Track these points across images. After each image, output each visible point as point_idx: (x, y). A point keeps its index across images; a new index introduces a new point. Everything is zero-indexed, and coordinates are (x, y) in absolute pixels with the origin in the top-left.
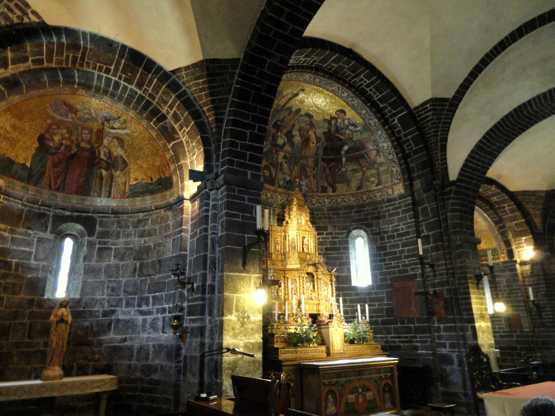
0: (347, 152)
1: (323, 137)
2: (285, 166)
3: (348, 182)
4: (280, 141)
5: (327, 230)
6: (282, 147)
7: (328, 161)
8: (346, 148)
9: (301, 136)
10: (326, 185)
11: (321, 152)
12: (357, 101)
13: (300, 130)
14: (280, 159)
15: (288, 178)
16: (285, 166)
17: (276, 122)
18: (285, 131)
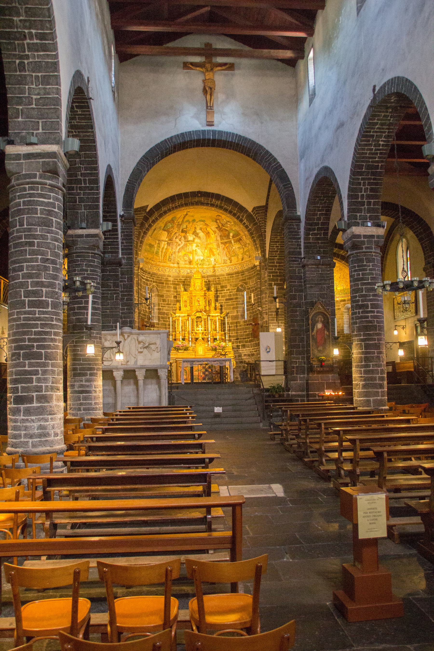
0: (233, 237)
1: (216, 230)
2: (199, 251)
8: (231, 235)
9: (203, 232)
11: (219, 238)
12: (221, 211)
15: (202, 258)
16: (199, 251)
17: (182, 230)
18: (191, 232)
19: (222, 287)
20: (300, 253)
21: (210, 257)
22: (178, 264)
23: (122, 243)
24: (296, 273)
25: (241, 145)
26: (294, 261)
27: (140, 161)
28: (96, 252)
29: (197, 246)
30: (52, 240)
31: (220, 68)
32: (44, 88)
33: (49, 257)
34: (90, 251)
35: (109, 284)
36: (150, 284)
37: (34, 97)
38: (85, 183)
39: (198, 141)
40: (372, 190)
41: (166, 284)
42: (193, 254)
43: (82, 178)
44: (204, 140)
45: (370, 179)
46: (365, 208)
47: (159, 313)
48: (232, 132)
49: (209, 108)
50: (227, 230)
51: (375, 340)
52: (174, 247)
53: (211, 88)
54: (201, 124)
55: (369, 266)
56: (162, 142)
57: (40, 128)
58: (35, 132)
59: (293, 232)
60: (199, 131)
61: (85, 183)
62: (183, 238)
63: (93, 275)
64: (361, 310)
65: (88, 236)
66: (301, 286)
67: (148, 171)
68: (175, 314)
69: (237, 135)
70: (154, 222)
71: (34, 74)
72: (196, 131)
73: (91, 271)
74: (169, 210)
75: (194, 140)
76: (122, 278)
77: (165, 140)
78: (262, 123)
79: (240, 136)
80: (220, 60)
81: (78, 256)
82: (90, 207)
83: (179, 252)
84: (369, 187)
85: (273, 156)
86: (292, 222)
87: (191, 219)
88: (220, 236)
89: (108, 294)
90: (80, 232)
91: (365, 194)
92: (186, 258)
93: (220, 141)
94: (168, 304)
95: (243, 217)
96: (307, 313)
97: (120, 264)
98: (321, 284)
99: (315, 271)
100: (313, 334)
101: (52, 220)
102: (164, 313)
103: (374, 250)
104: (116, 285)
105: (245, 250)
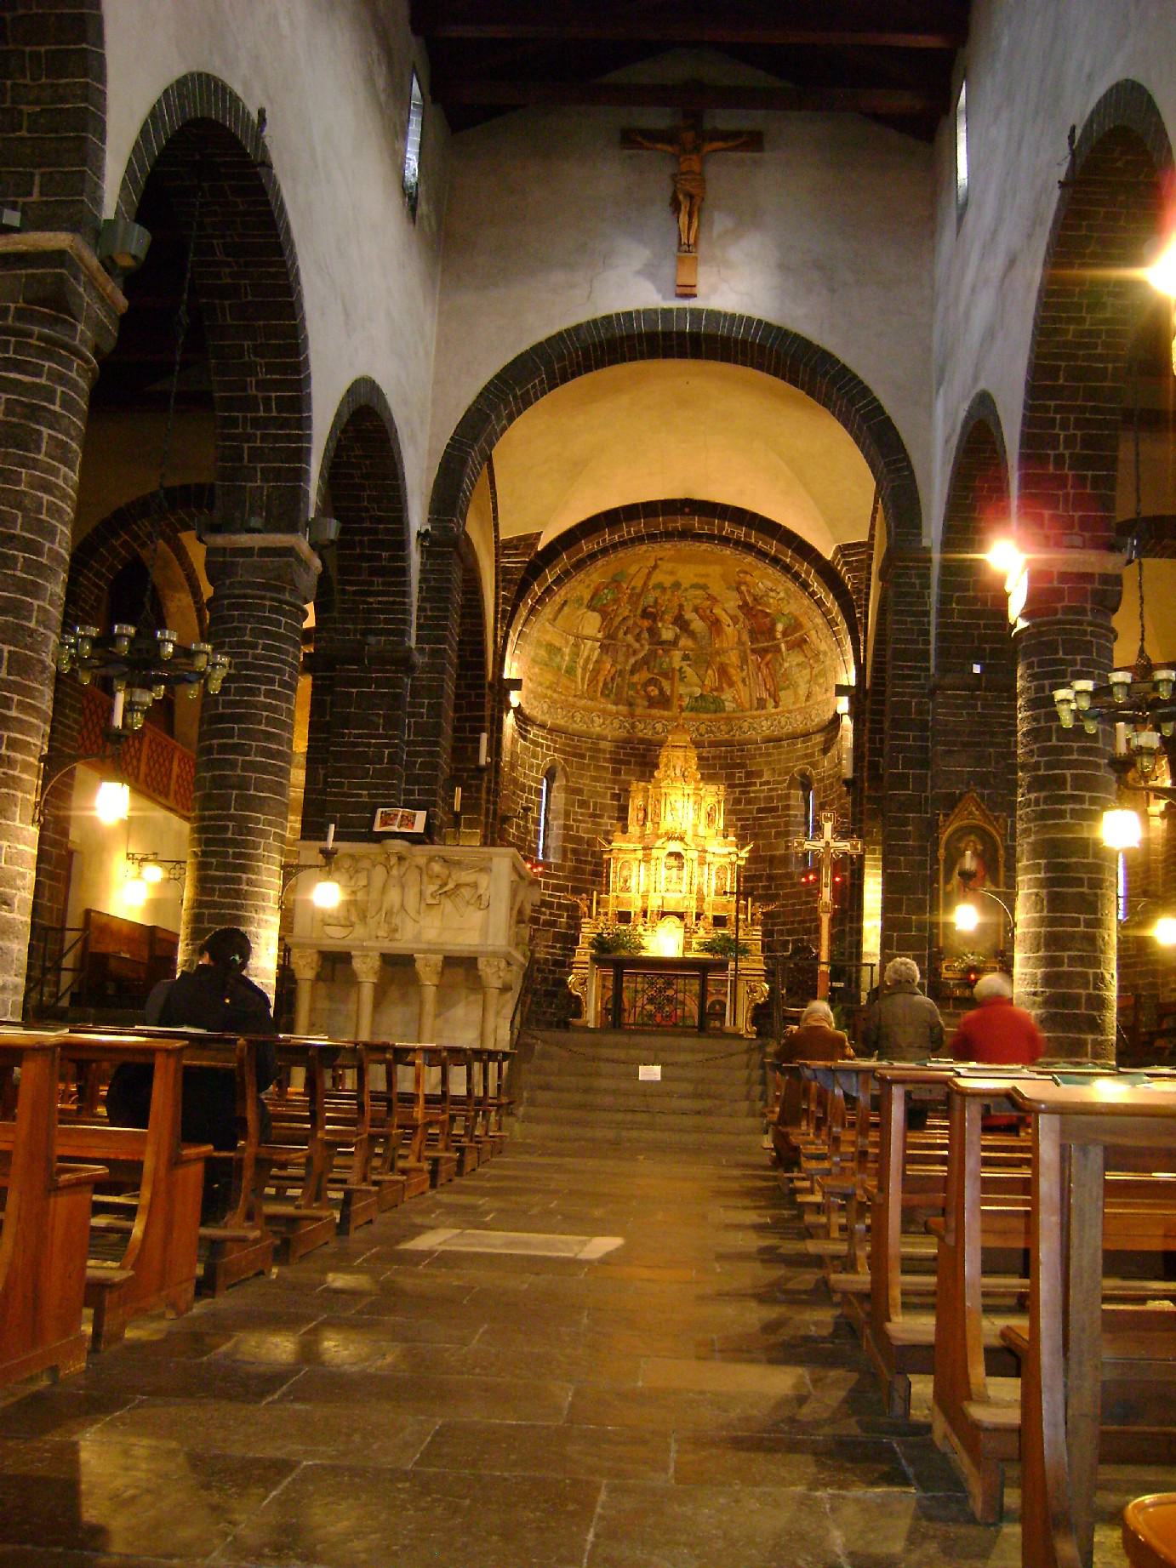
0: (785, 634)
2: (689, 671)
3: (796, 686)
4: (667, 634)
5: (761, 776)
6: (674, 643)
7: (762, 652)
8: (780, 627)
9: (701, 618)
10: (765, 695)
11: (745, 637)
13: (696, 610)
14: (677, 665)
15: (698, 691)
16: (689, 671)
17: (644, 611)
18: (668, 617)
19: (749, 775)
20: (925, 656)
21: (720, 689)
22: (630, 705)
23: (420, 609)
24: (909, 713)
25: (753, 343)
26: (909, 677)
27: (486, 388)
28: (287, 597)
29: (686, 658)
30: (32, 487)
31: (720, 144)
32: (52, 85)
33: (17, 532)
34: (268, 594)
35: (375, 719)
36: (545, 756)
37: (26, 109)
38: (268, 409)
39: (652, 337)
40: (1087, 442)
41: (591, 758)
42: (672, 679)
43: (260, 395)
44: (667, 335)
45: (1083, 409)
46: (1066, 495)
47: (567, 838)
48: (747, 313)
49: (687, 250)
50: (767, 615)
51: (1079, 882)
52: (621, 659)
53: (691, 197)
54: (659, 290)
55: (1074, 663)
56: (549, 340)
57: (36, 190)
58: (21, 200)
59: (906, 594)
60: (655, 311)
61: (268, 409)
62: (646, 635)
63: (271, 659)
64: (1043, 794)
65: (266, 551)
66: (924, 749)
67: (511, 419)
68: (610, 843)
69: (760, 322)
70: (558, 581)
71: (28, 49)
72: (647, 312)
73: (266, 647)
74: (604, 551)
75: (640, 335)
76: (412, 705)
77: (560, 334)
78: (833, 290)
79: (767, 324)
80: (725, 119)
81: (233, 607)
82: (278, 474)
83: (632, 672)
84: (1079, 433)
85: (861, 382)
86: (907, 567)
87: (668, 581)
88: (751, 632)
89: (369, 745)
90: (244, 540)
91: (1067, 453)
92: (654, 691)
93: (712, 338)
94: (593, 816)
95: (808, 574)
96: (932, 827)
97: (405, 663)
98: (978, 744)
99: (964, 707)
100: (949, 887)
101: (40, 433)
102: (579, 840)
103: (1089, 618)
104: (393, 723)
105: (815, 671)
